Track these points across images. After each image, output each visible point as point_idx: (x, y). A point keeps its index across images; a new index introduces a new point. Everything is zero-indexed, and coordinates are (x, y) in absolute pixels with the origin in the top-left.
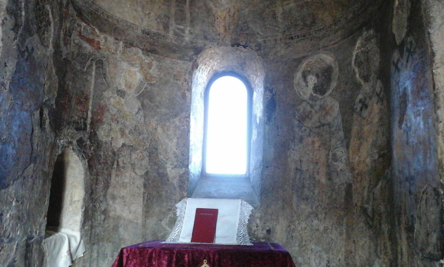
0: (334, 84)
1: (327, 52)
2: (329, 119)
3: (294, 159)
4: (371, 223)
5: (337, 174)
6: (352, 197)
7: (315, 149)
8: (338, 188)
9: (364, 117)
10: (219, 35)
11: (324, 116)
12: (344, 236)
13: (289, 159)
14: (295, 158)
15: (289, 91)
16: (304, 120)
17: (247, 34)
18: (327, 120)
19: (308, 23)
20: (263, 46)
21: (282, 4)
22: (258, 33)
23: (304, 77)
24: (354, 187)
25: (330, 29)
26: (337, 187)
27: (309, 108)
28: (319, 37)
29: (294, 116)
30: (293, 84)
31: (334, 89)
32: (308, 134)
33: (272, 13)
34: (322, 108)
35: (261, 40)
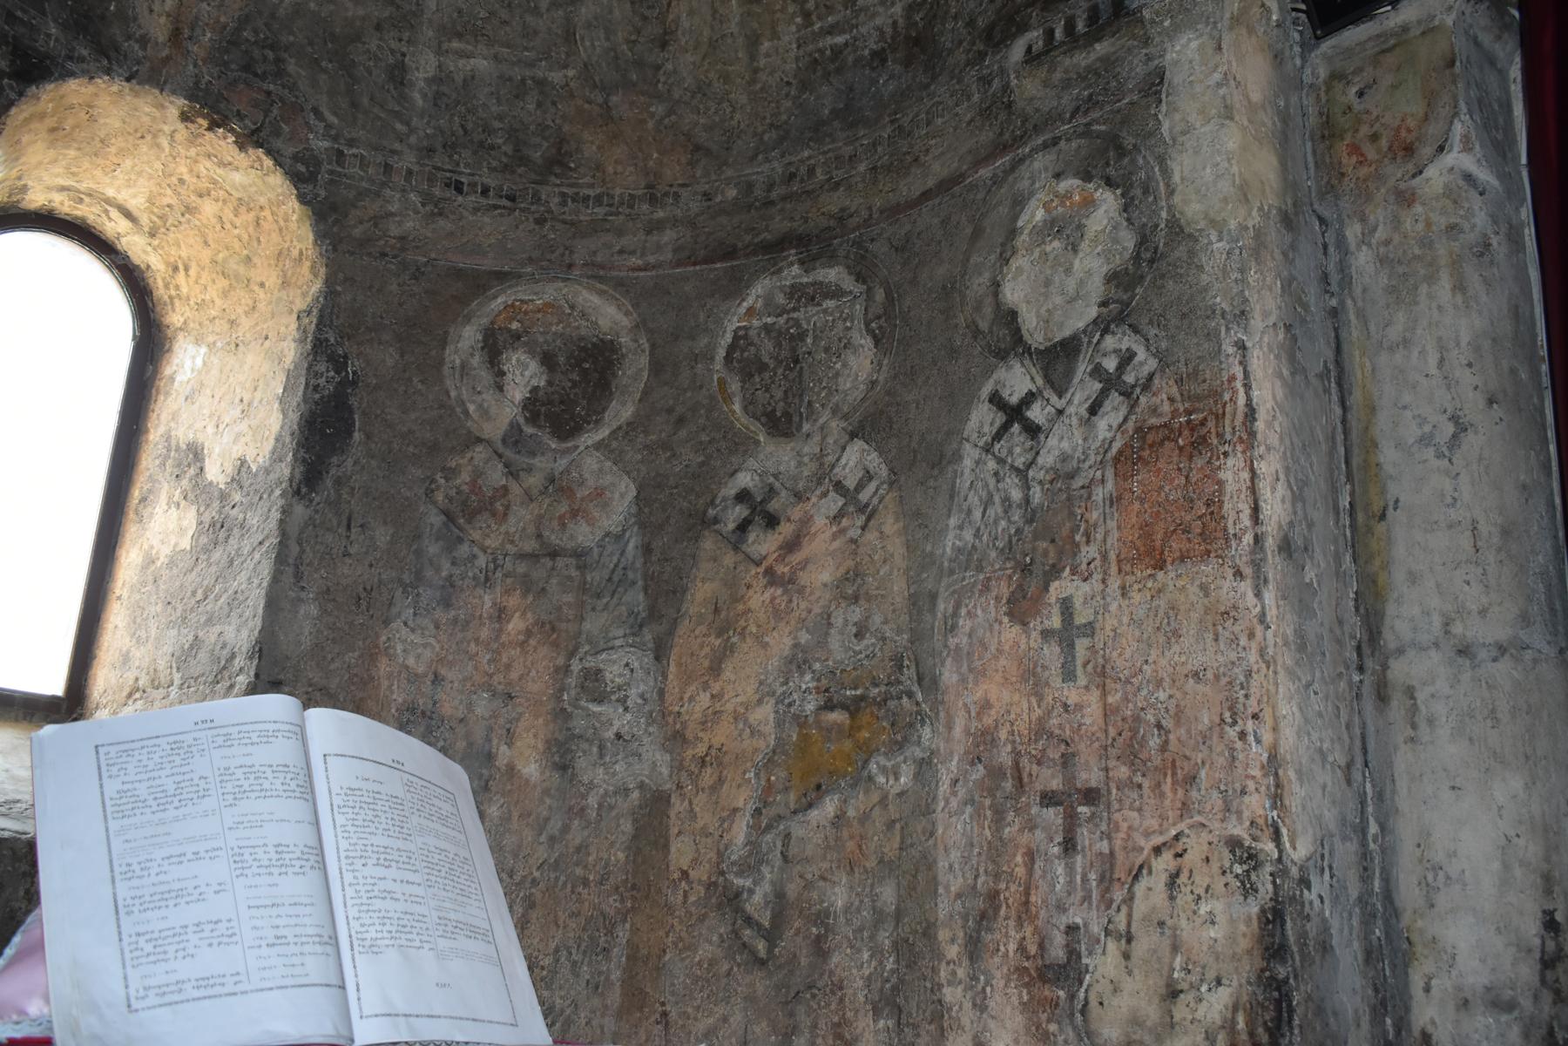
0: (621, 411)
1: (604, 287)
2: (584, 534)
3: (407, 667)
4: (761, 947)
5: (601, 748)
6: (666, 847)
7: (504, 638)
8: (600, 805)
9: (756, 556)
10: (144, 41)
11: (561, 517)
12: (615, 997)
13: (383, 666)
14: (411, 661)
15: (420, 386)
16: (472, 516)
17: (269, 93)
18: (572, 537)
19: (537, 155)
20: (331, 172)
21: (440, 43)
22: (316, 111)
23: (493, 347)
24: (678, 806)
25: (627, 211)
26: (592, 801)
27: (496, 476)
28: (572, 224)
29: (429, 493)
30: (441, 362)
31: (620, 428)
32: (482, 577)
33: (391, 60)
34: (557, 486)
35: (326, 144)
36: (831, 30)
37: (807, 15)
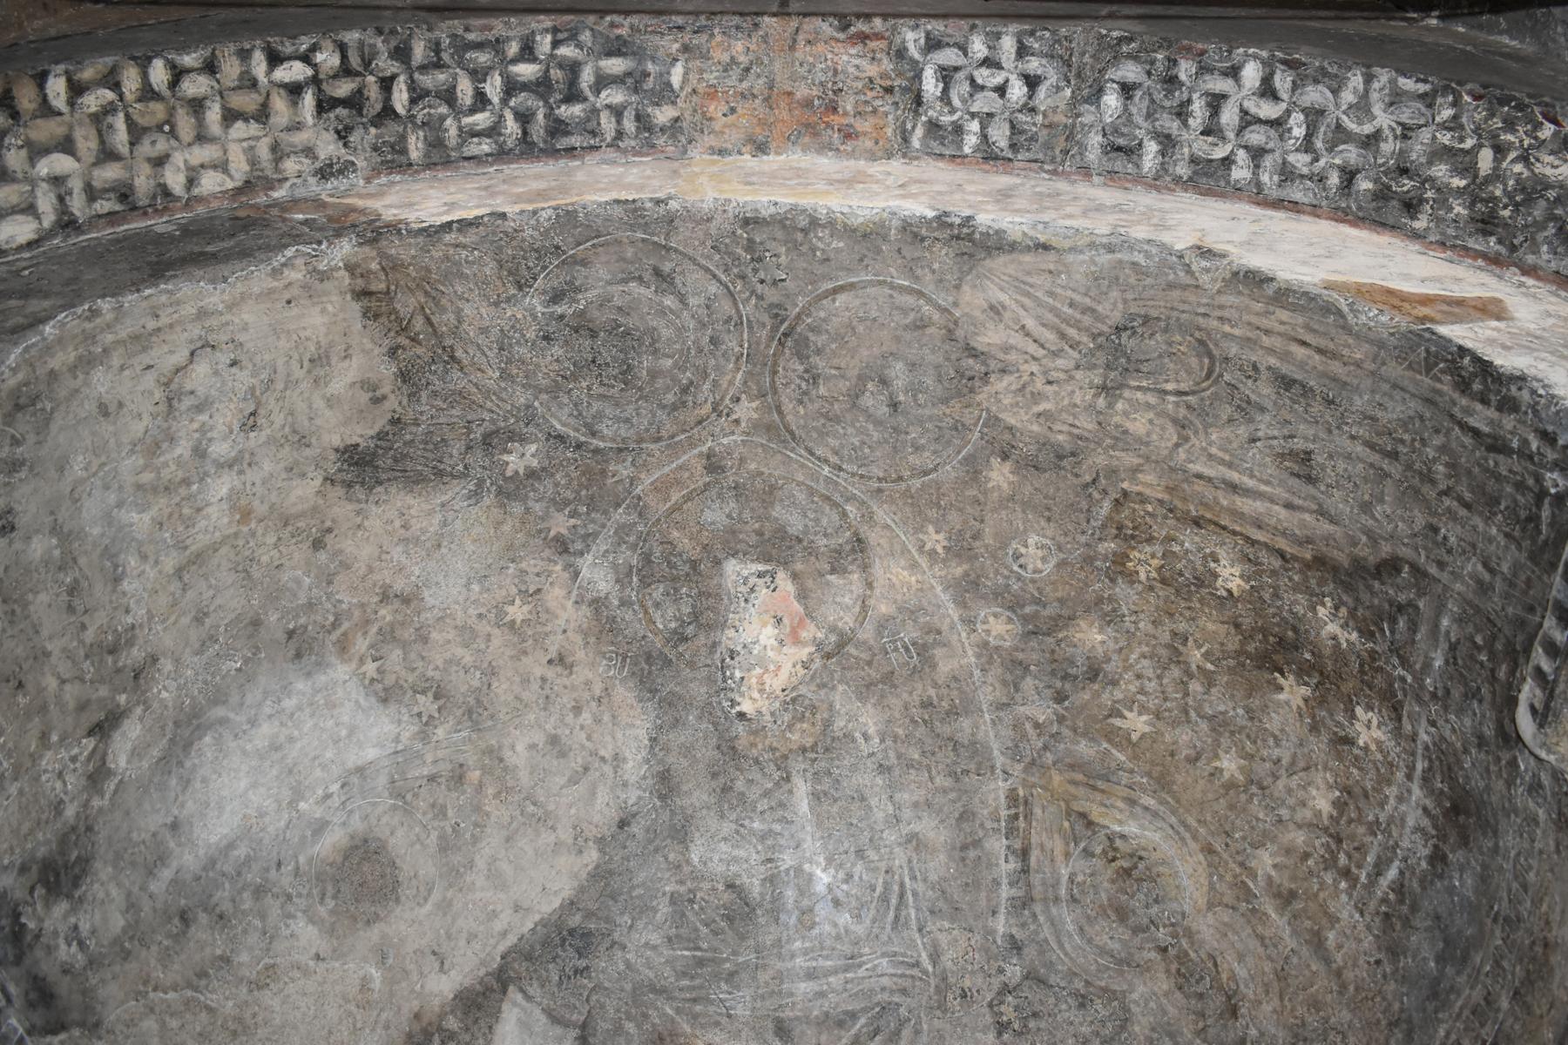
36: (1379, 870)
37: (1346, 873)
